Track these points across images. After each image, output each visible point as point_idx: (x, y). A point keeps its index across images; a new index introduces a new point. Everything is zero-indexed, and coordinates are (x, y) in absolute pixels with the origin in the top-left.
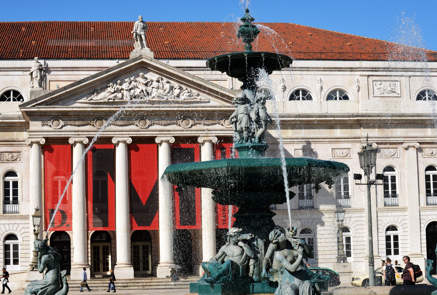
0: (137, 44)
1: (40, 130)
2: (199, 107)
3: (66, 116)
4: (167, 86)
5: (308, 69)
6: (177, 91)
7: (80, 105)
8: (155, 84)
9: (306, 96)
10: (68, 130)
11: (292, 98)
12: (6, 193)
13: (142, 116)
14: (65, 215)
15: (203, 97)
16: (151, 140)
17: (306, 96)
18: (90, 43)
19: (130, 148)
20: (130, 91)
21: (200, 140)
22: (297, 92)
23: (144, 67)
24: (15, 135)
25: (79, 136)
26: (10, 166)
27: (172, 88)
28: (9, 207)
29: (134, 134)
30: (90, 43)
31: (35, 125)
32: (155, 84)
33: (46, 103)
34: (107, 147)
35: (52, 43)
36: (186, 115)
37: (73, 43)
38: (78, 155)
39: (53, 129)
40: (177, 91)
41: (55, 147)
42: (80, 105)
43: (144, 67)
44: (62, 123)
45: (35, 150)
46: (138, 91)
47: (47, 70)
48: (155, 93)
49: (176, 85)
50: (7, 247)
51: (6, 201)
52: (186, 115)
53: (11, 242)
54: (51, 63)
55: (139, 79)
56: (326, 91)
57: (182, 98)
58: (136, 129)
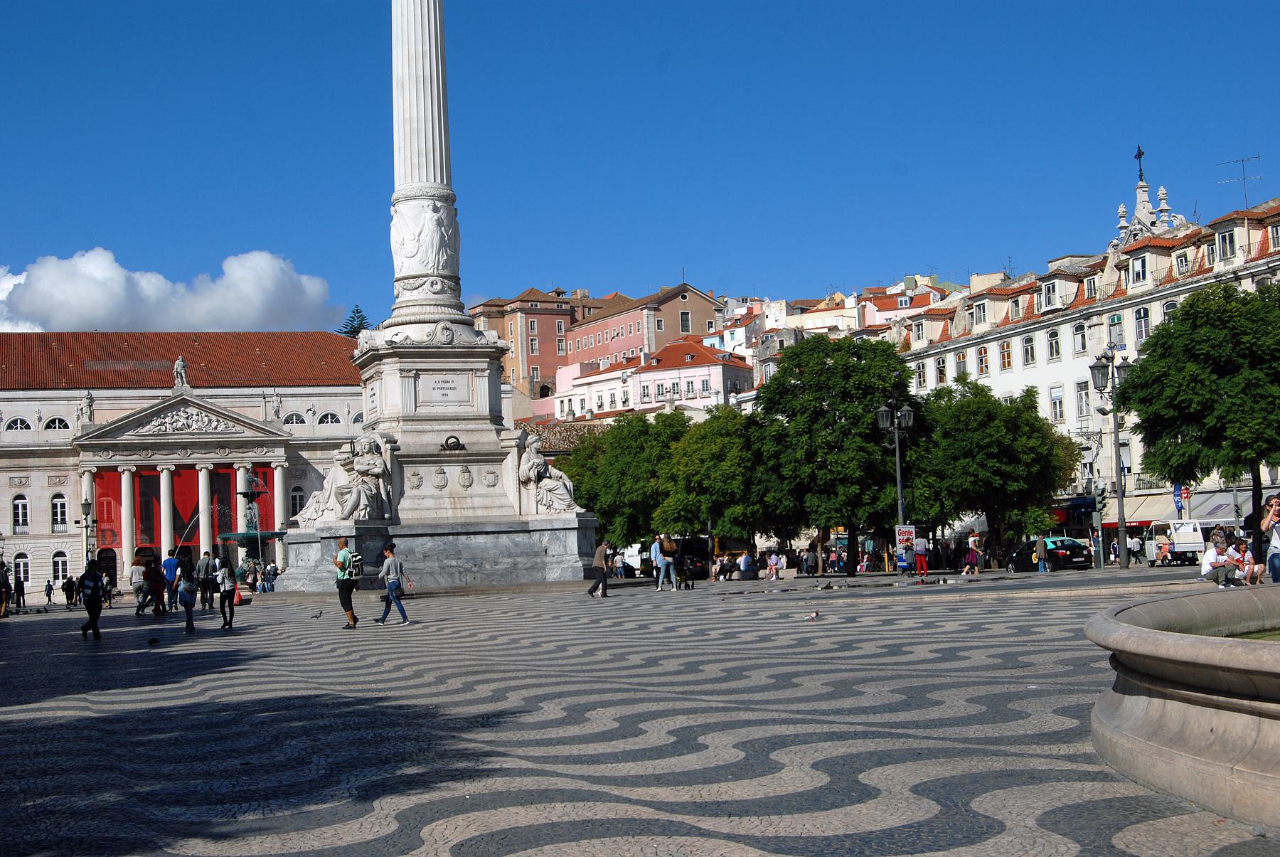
0: (178, 381)
1: (92, 460)
2: (234, 438)
3: (115, 448)
4: (206, 419)
5: (336, 395)
6: (214, 424)
7: (128, 437)
9: (335, 419)
10: (117, 460)
11: (321, 421)
12: (55, 514)
13: (184, 446)
14: (116, 534)
15: (238, 428)
16: (192, 466)
17: (335, 419)
18: (127, 366)
19: (173, 475)
20: (170, 424)
21: (235, 466)
22: (326, 416)
23: (185, 403)
24: (62, 460)
25: (126, 465)
26: (57, 490)
27: (210, 421)
28: (57, 527)
29: (177, 462)
30: (127, 366)
31: (85, 456)
33: (97, 437)
34: (152, 473)
35: (91, 366)
36: (222, 445)
37: (110, 366)
38: (125, 481)
39: (103, 459)
40: (214, 424)
41: (105, 475)
42: (128, 437)
43: (185, 403)
44: (111, 453)
45: (86, 479)
46: (180, 424)
47: (92, 400)
48: (195, 426)
49: (214, 418)
50: (56, 564)
51: (55, 521)
52: (222, 445)
53: (60, 559)
54: (95, 393)
55: (181, 413)
56: (353, 415)
57: (219, 429)
58: (178, 458)
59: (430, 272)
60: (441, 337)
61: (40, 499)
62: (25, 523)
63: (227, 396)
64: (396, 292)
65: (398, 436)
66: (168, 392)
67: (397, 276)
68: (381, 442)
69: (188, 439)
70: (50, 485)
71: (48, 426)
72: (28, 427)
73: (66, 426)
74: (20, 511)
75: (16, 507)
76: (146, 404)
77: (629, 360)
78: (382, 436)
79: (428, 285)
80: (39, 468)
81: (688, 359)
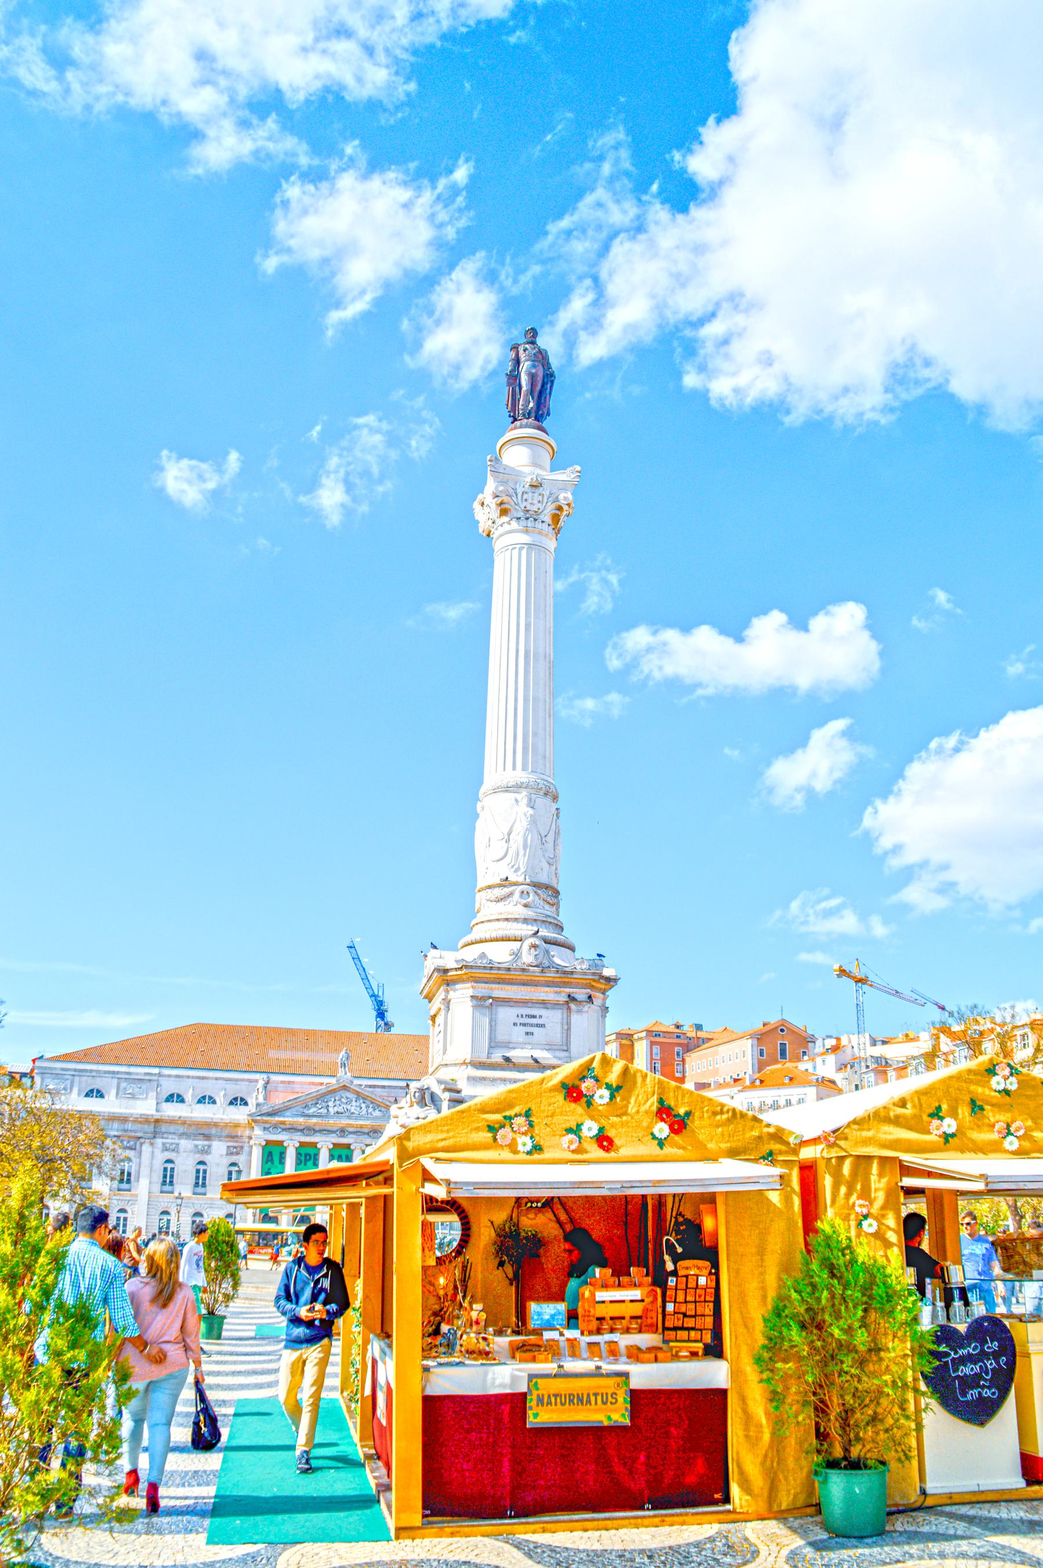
8: (354, 1103)
26: (234, 1159)
32: (354, 1103)
33: (269, 1114)
54: (274, 1078)
59: (521, 879)
60: (528, 958)
61: (218, 1165)
62: (204, 1185)
63: (384, 1087)
64: (477, 906)
65: (462, 1084)
66: (333, 1081)
67: (481, 884)
68: (437, 1089)
69: (344, 1122)
70: (227, 1154)
71: (231, 1103)
72: (214, 1102)
73: (246, 1104)
74: (201, 1174)
75: (198, 1171)
76: (314, 1089)
77: (736, 1080)
78: (440, 1082)
79: (517, 895)
80: (219, 1138)
81: (787, 1080)
